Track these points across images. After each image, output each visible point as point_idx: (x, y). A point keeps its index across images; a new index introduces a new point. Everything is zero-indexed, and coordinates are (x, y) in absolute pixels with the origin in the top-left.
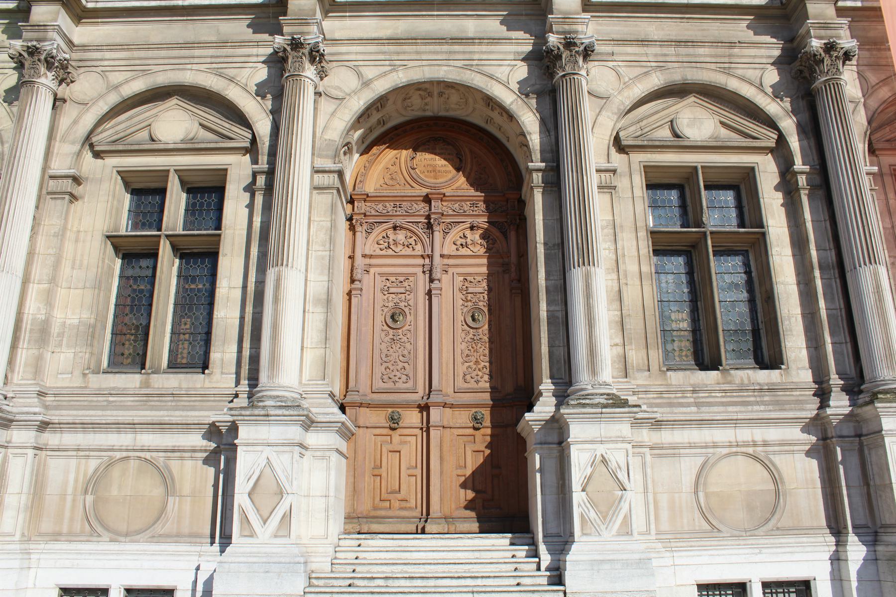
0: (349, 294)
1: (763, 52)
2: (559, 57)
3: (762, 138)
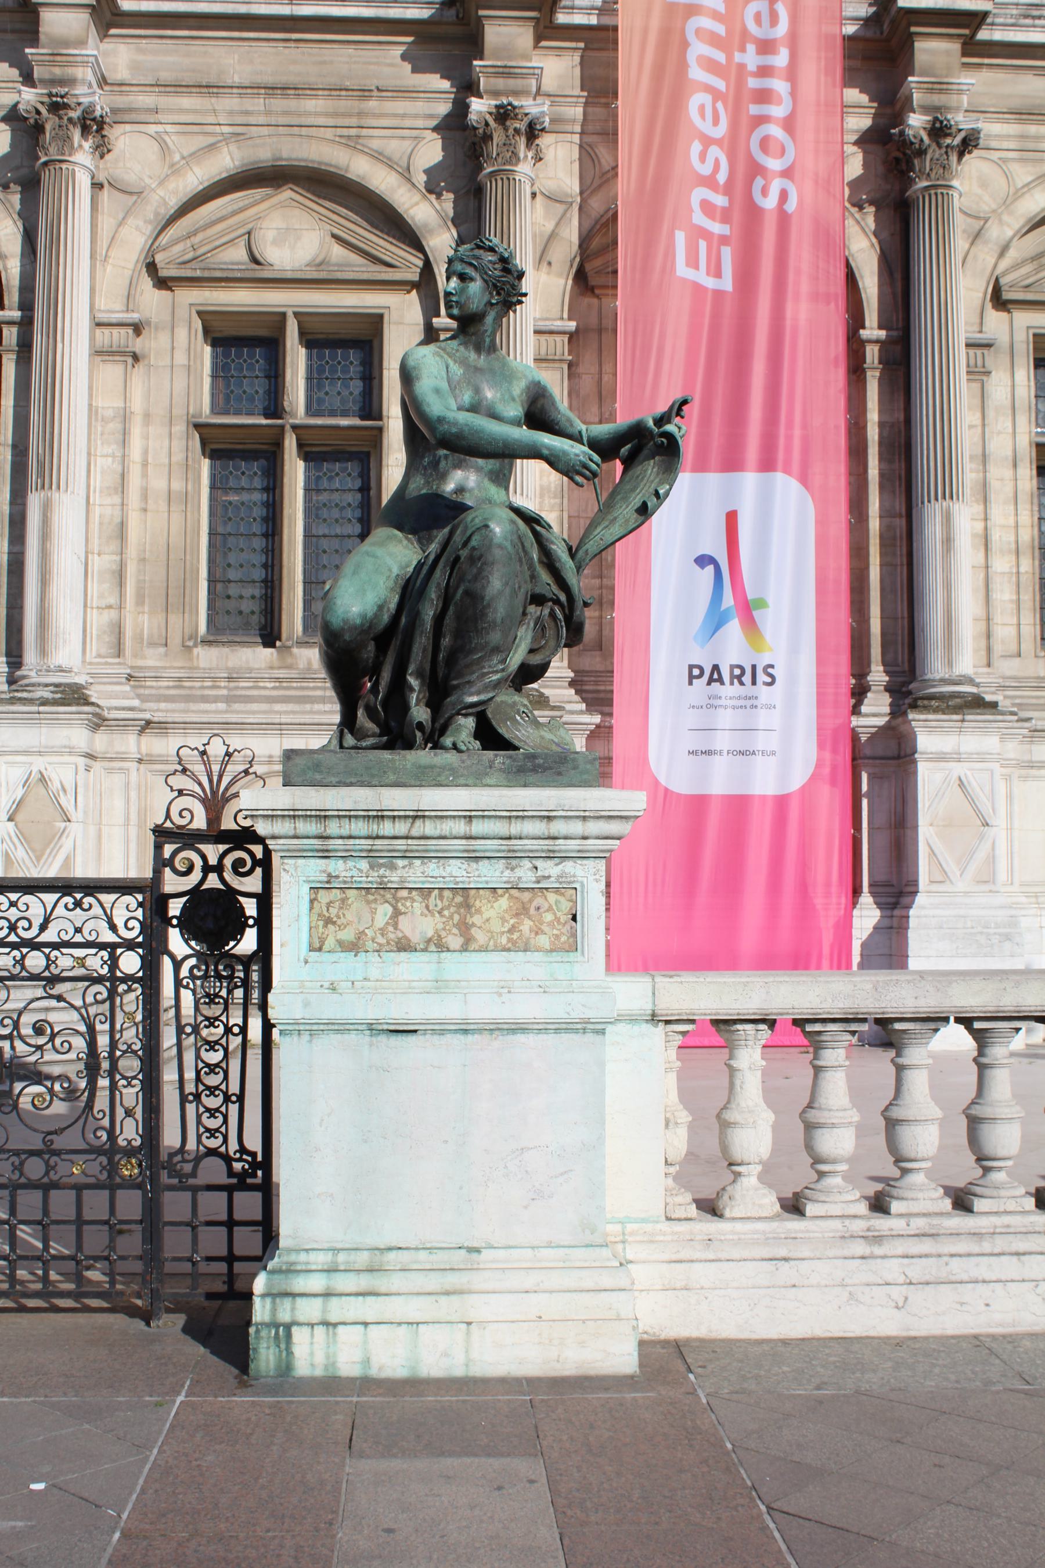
1: (420, 107)
3: (398, 264)
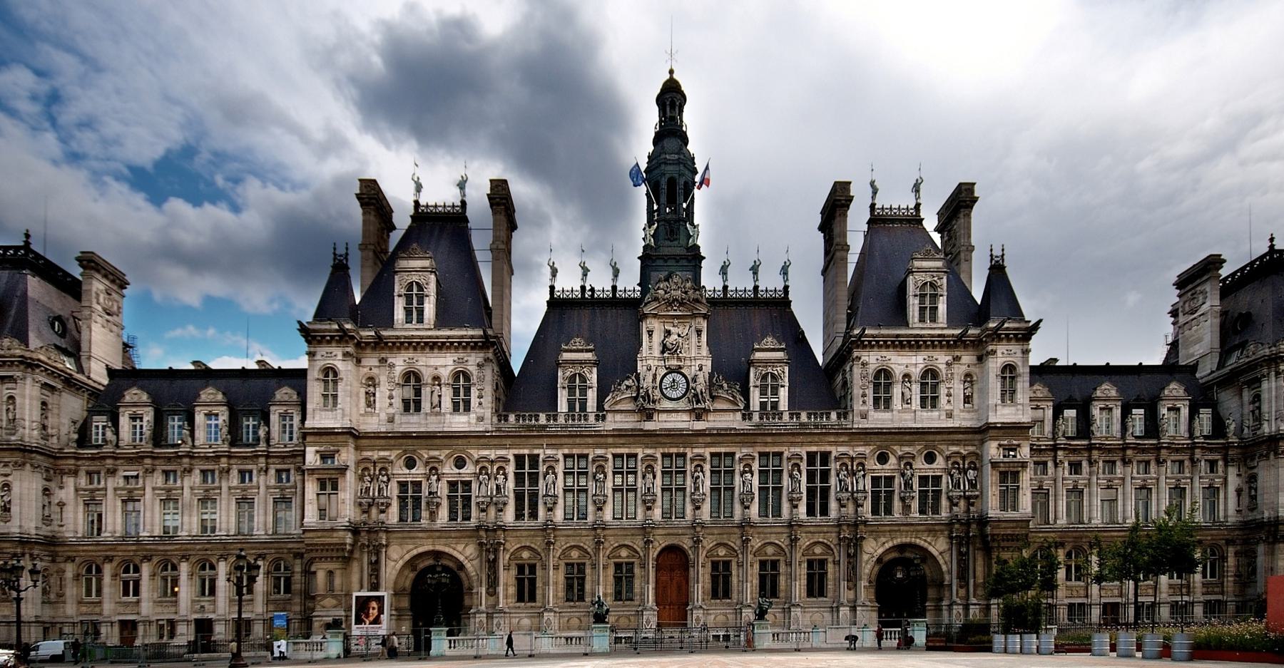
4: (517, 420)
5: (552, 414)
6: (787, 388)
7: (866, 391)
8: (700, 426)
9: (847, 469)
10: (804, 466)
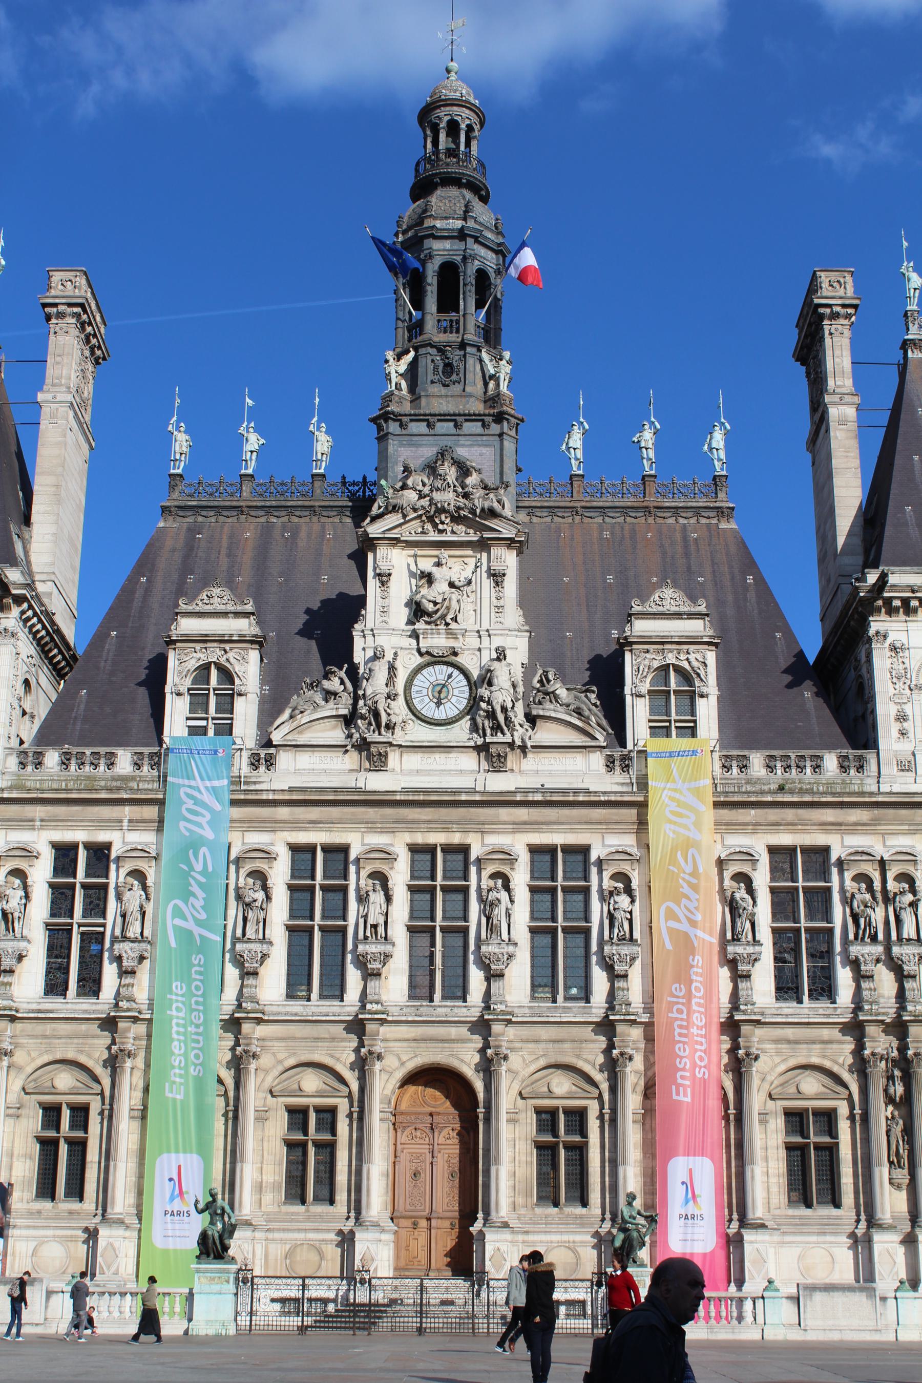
0: (394, 1163)
1: (597, 1045)
2: (492, 1060)
4: (65, 763)
5: (146, 750)
6: (713, 700)
7: (908, 709)
8: (499, 783)
9: (870, 889)
10: (762, 879)
